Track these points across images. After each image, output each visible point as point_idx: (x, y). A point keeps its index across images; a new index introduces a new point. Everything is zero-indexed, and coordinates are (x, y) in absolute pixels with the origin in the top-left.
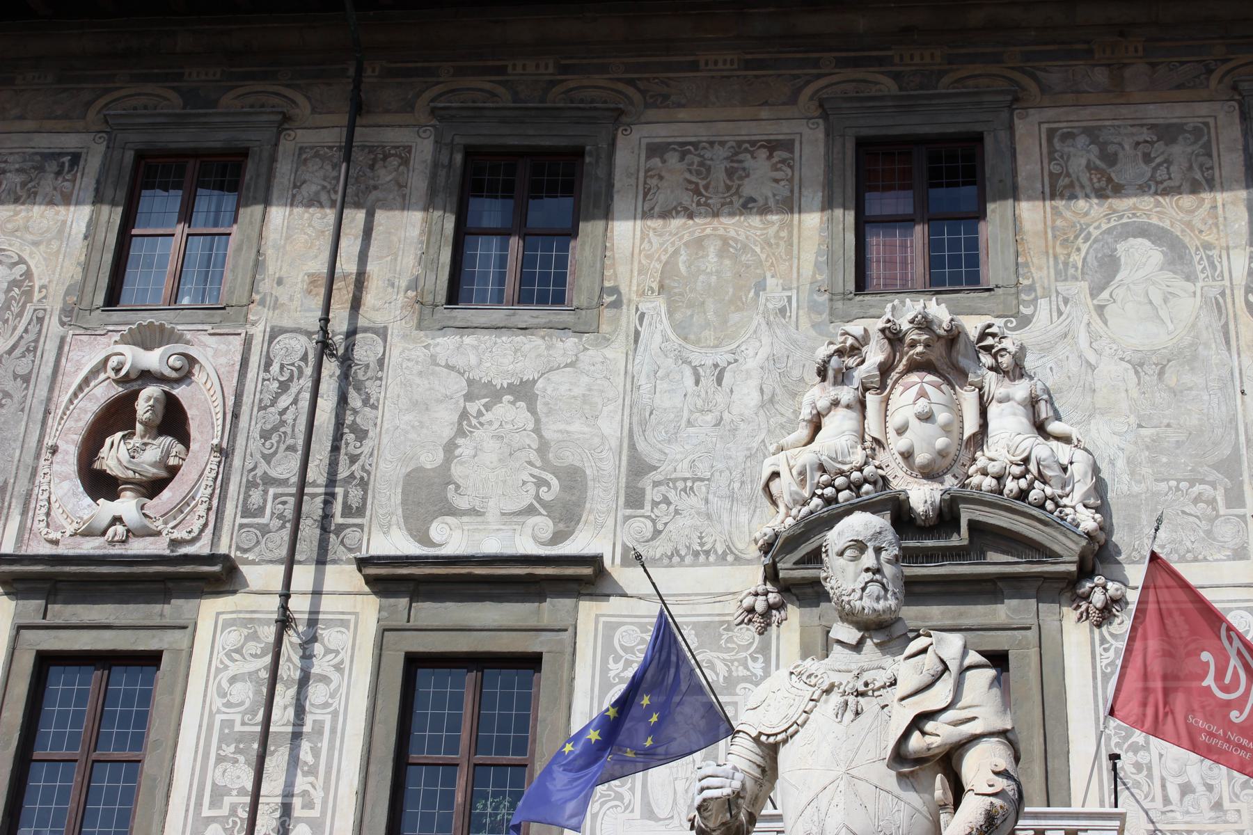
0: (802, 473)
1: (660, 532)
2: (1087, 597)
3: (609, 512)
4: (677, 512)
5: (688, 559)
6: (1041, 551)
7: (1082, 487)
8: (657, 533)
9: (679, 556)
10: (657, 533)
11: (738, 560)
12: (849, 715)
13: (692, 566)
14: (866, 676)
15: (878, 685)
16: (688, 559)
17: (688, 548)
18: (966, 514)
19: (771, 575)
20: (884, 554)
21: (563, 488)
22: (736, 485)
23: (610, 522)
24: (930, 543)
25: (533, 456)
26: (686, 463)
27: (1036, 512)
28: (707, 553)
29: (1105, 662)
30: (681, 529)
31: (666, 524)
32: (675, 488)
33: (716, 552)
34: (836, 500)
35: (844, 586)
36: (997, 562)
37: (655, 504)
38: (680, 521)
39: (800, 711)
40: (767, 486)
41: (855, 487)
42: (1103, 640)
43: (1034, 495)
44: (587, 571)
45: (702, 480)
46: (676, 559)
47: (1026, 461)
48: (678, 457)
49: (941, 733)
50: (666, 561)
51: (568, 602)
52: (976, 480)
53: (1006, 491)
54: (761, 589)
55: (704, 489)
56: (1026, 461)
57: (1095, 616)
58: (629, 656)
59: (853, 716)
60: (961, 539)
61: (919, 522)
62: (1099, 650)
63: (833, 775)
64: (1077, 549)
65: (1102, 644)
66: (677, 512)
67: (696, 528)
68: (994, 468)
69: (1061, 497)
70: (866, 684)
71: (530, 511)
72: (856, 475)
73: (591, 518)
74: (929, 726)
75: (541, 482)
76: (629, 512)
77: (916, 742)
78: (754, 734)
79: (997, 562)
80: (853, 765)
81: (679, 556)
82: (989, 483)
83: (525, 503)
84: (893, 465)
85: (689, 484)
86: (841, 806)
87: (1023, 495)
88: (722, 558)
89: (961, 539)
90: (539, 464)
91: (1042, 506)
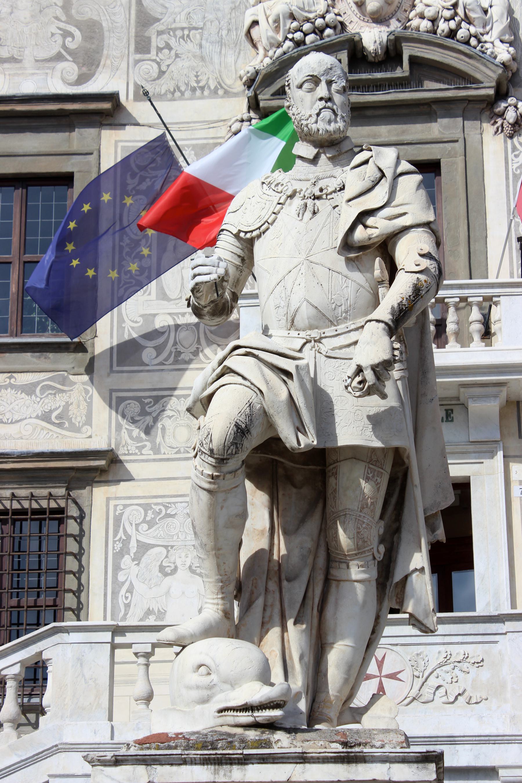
0: (277, 21)
1: (164, 73)
2: (502, 115)
3: (122, 57)
4: (177, 56)
5: (188, 94)
6: (465, 79)
7: (499, 25)
8: (162, 73)
9: (180, 91)
10: (162, 73)
11: (227, 93)
12: (308, 214)
13: (191, 99)
14: (321, 184)
15: (330, 190)
16: (188, 94)
17: (187, 85)
18: (408, 51)
19: (254, 104)
20: (334, 86)
21: (85, 38)
22: (224, 33)
23: (124, 65)
24: (379, 75)
25: (59, 12)
26: (183, 16)
27: (463, 48)
28: (202, 88)
29: (515, 166)
30: (181, 69)
31: (168, 66)
32: (175, 36)
33: (209, 88)
34: (303, 42)
35: (303, 113)
36: (432, 89)
37: (159, 50)
38: (180, 63)
39: (270, 212)
40: (248, 32)
41: (319, 31)
42: (514, 149)
43: (461, 34)
44: (106, 106)
45: (196, 29)
46: (178, 94)
47: (455, 6)
48: (177, 10)
49: (379, 226)
50: (169, 96)
51: (91, 132)
52: (415, 22)
53: (439, 31)
54: (245, 116)
55: (198, 36)
56: (455, 6)
57: (508, 130)
58: (142, 173)
59: (311, 215)
60: (403, 71)
61: (370, 59)
62: (511, 156)
63: (296, 261)
64: (495, 76)
65: (513, 151)
66: (177, 56)
67: (193, 68)
68: (429, 13)
69: (482, 35)
70: (321, 190)
71: (59, 57)
72: (319, 22)
73: (108, 62)
74: (370, 221)
75: (66, 34)
76: (138, 56)
77: (360, 233)
78: (235, 232)
79: (432, 89)
80: (311, 253)
81: (180, 91)
82: (425, 25)
83: (53, 52)
84: (349, 12)
85: (186, 32)
86: (303, 285)
87: (452, 34)
88: (214, 93)
89: (403, 71)
90: (64, 18)
91: (467, 43)
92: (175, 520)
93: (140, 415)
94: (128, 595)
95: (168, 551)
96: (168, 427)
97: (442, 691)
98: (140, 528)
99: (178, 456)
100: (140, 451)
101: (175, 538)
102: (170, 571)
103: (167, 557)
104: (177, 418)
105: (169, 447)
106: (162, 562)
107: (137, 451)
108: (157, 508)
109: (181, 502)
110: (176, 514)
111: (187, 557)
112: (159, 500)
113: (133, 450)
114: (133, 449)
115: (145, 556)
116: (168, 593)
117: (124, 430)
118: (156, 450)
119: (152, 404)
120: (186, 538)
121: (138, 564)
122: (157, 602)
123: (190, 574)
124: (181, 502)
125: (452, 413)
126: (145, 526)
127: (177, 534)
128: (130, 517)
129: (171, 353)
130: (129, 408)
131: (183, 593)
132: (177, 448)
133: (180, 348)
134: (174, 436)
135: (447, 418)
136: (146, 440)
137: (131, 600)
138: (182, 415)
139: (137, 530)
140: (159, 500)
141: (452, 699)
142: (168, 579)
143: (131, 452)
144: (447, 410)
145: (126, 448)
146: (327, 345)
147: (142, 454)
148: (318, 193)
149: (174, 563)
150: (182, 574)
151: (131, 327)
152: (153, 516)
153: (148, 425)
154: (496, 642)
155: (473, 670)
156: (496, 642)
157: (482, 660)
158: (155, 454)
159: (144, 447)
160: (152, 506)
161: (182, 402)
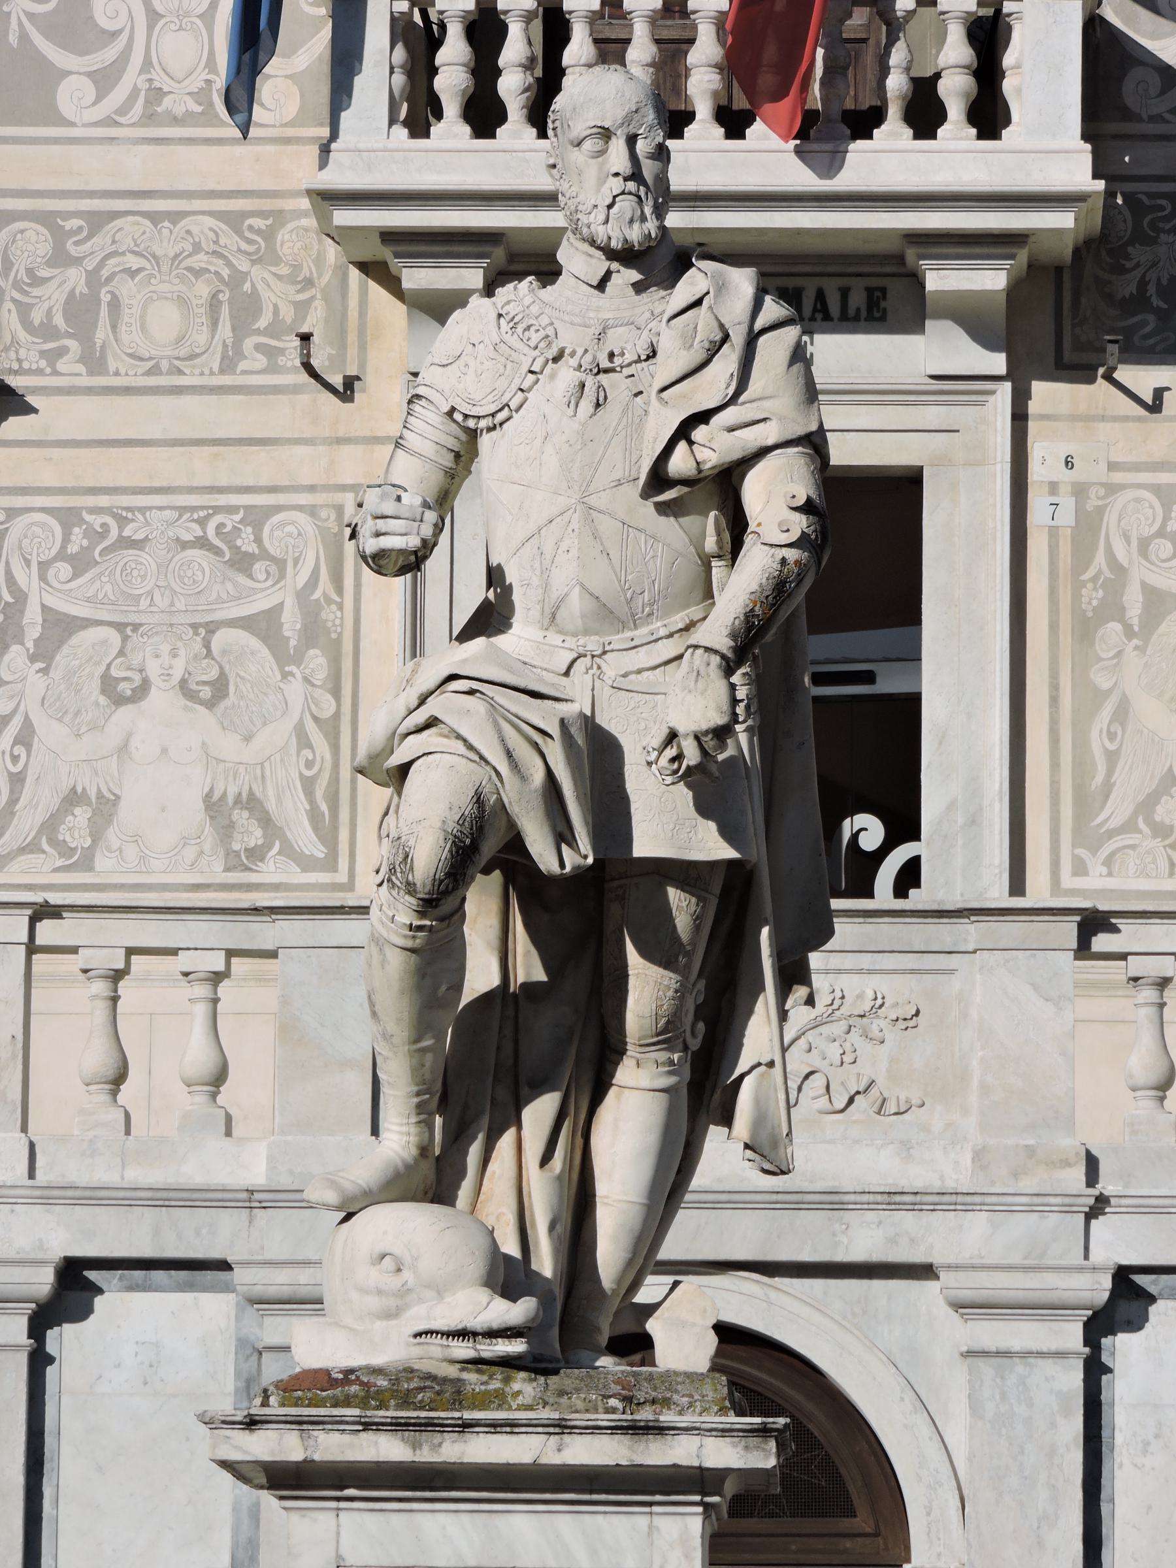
12: (586, 406)
14: (613, 342)
15: (629, 357)
35: (581, 198)
39: (514, 387)
59: (592, 410)
70: (611, 356)
74: (700, 433)
77: (680, 463)
80: (591, 489)
86: (574, 553)
92: (144, 556)
93: (51, 263)
94: (20, 750)
95: (125, 638)
96: (127, 301)
97: (817, 1082)
98: (51, 573)
99: (152, 381)
100: (52, 364)
101: (144, 603)
102: (129, 693)
103: (121, 653)
104: (151, 276)
105: (131, 355)
106: (109, 665)
107: (43, 364)
108: (96, 521)
109: (161, 508)
110: (146, 539)
111: (175, 656)
112: (103, 501)
113: (33, 359)
114: (33, 359)
115: (65, 650)
116: (123, 750)
117: (9, 305)
118: (95, 362)
119: (85, 234)
120: (172, 604)
121: (45, 671)
122: (97, 774)
123: (184, 702)
124: (161, 508)
125: (884, 298)
126: (63, 569)
127: (150, 593)
128: (25, 542)
129: (135, 91)
130: (20, 243)
131: (164, 751)
132: (151, 358)
133: (162, 81)
134: (143, 327)
135: (870, 310)
136: (68, 335)
137: (26, 765)
138: (165, 268)
139: (43, 578)
140: (103, 501)
141: (840, 1103)
142: (124, 714)
143: (26, 365)
144: (869, 290)
145: (13, 355)
146: (613, 666)
147: (55, 373)
148: (605, 364)
149: (141, 671)
150: (161, 699)
151: (27, 14)
152: (85, 543)
153: (73, 290)
154: (952, 971)
155: (892, 1036)
156: (952, 971)
157: (917, 1013)
158: (91, 373)
159: (62, 352)
160: (85, 514)
161: (166, 232)
